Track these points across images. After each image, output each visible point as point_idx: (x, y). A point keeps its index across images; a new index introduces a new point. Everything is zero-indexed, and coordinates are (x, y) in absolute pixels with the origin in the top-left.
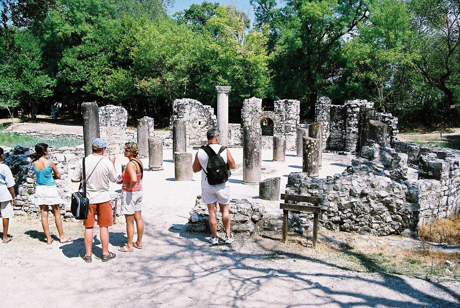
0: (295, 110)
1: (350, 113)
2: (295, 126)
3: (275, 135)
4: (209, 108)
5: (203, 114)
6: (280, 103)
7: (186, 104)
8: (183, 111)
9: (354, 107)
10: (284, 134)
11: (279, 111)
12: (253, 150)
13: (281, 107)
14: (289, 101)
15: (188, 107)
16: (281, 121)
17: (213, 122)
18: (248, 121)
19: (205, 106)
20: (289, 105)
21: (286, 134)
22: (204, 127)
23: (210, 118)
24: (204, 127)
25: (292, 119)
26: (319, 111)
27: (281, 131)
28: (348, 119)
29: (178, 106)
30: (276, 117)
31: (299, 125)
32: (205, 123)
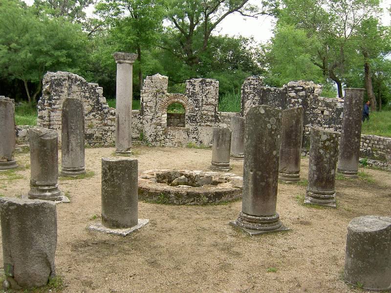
0: (214, 93)
1: (293, 98)
2: (213, 114)
3: (187, 126)
4: (96, 86)
5: (87, 95)
6: (195, 84)
7: (65, 80)
8: (58, 88)
9: (299, 91)
10: (200, 125)
11: (193, 94)
12: (272, 153)
13: (197, 89)
14: (208, 80)
15: (66, 83)
16: (196, 107)
17: (101, 107)
18: (151, 107)
19: (90, 84)
20: (206, 86)
21: (203, 124)
22: (89, 113)
23: (98, 102)
24: (89, 113)
25: (210, 104)
26: (249, 94)
27: (196, 120)
28: (291, 105)
29: (52, 83)
30: (190, 101)
31: (219, 112)
32: (90, 108)
